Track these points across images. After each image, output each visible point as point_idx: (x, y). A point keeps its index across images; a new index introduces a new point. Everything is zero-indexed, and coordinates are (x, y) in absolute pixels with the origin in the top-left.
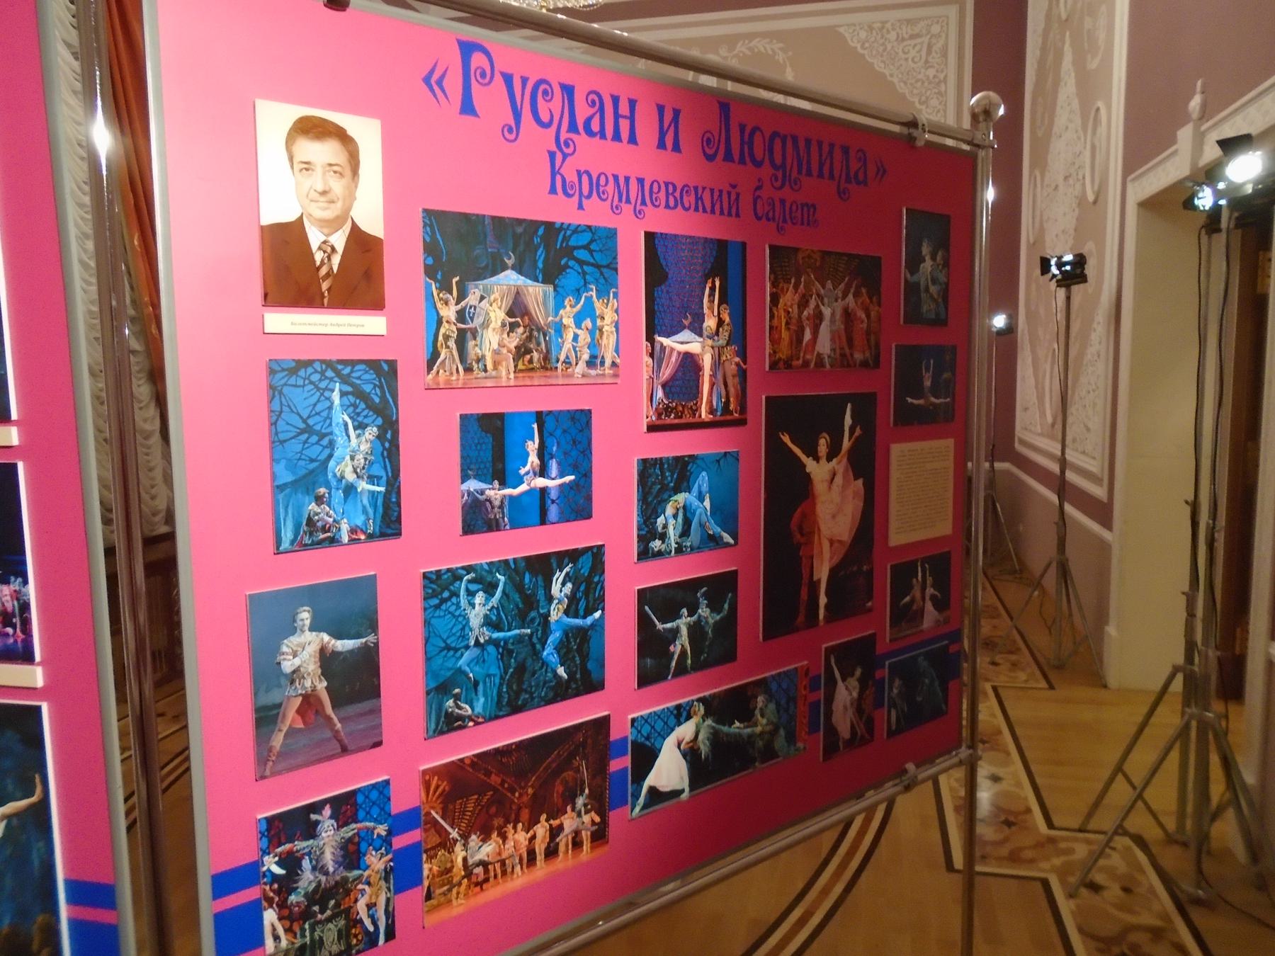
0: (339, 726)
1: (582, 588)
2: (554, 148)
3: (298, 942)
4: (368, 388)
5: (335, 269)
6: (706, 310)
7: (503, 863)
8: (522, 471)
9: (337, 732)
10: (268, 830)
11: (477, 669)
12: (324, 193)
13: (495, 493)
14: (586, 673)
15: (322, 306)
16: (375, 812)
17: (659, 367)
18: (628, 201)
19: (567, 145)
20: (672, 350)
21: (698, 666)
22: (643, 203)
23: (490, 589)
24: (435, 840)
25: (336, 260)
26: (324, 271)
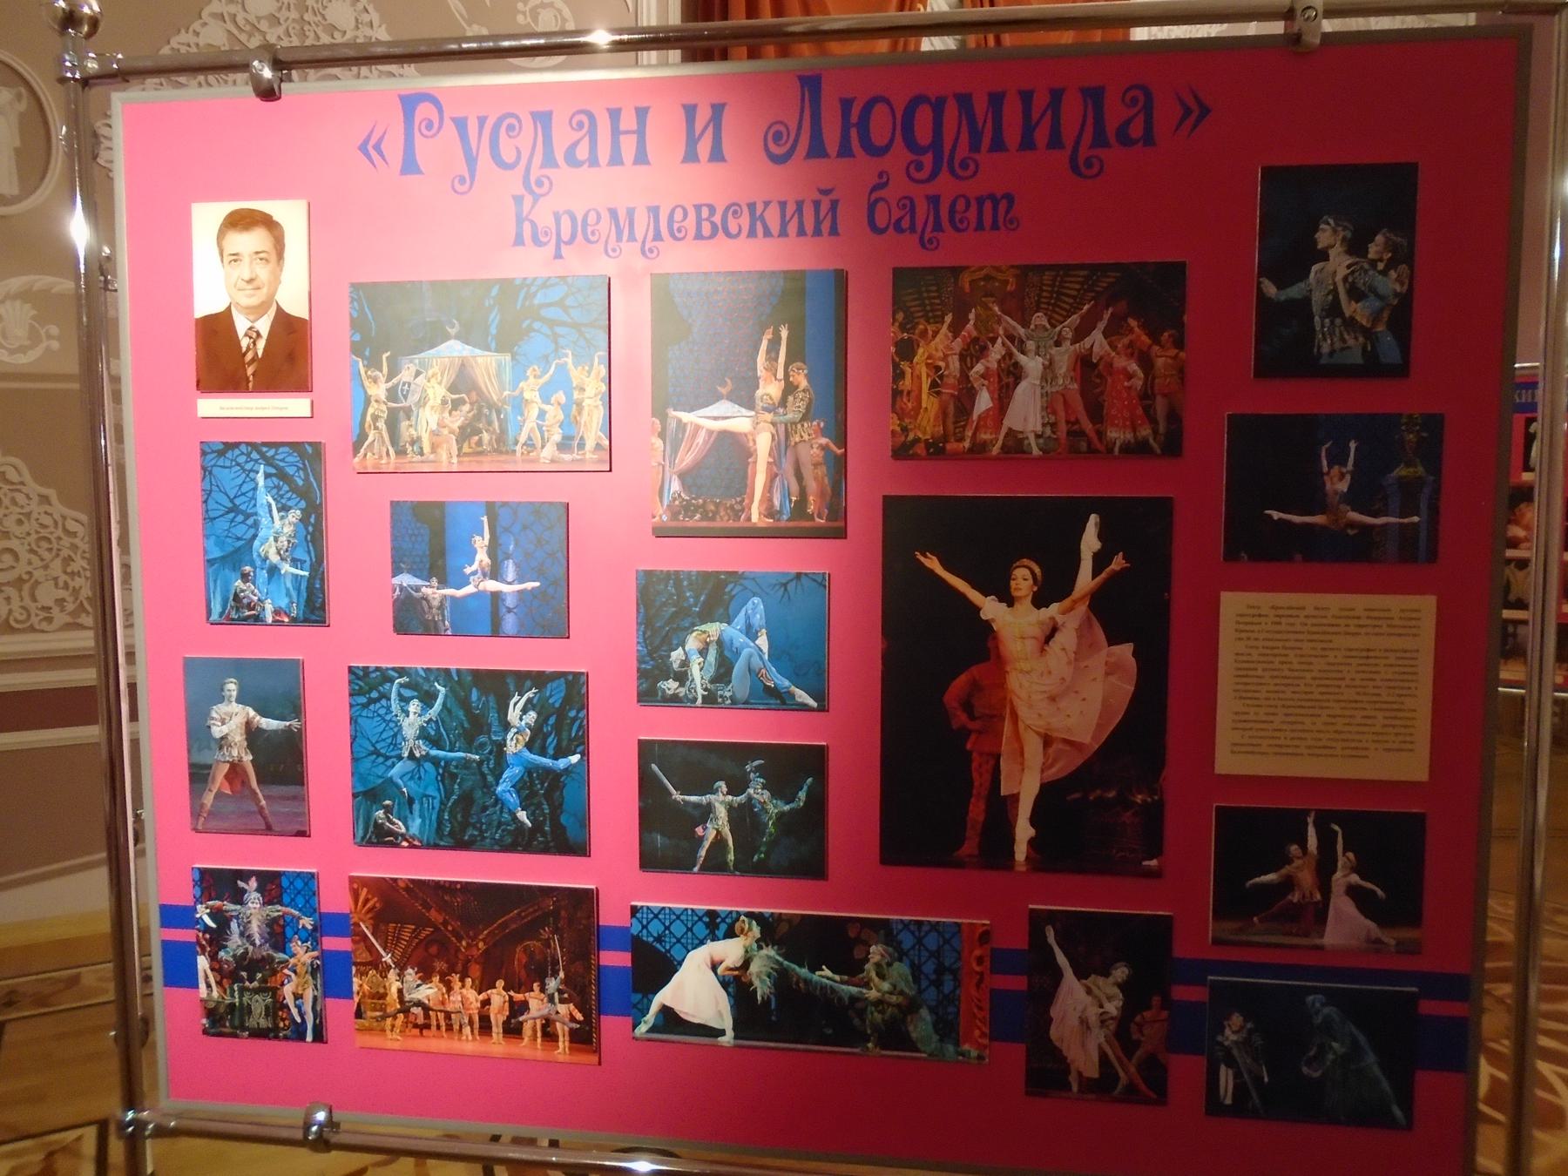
0: (263, 802)
1: (552, 720)
2: (520, 190)
3: (228, 1000)
4: (291, 470)
5: (260, 353)
6: (761, 371)
7: (448, 1015)
8: (468, 570)
9: (262, 808)
10: (202, 880)
11: (412, 784)
12: (250, 281)
13: (433, 592)
14: (559, 829)
15: (247, 390)
16: (300, 901)
17: (675, 451)
18: (632, 238)
19: (539, 184)
20: (698, 428)
21: (746, 867)
22: (938, 226)
23: (428, 699)
24: (364, 956)
25: (261, 345)
26: (249, 356)
